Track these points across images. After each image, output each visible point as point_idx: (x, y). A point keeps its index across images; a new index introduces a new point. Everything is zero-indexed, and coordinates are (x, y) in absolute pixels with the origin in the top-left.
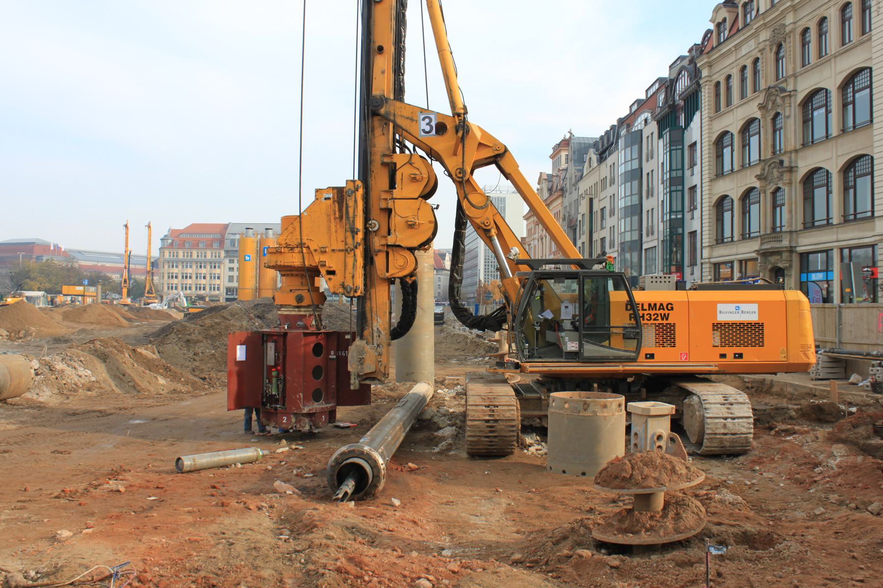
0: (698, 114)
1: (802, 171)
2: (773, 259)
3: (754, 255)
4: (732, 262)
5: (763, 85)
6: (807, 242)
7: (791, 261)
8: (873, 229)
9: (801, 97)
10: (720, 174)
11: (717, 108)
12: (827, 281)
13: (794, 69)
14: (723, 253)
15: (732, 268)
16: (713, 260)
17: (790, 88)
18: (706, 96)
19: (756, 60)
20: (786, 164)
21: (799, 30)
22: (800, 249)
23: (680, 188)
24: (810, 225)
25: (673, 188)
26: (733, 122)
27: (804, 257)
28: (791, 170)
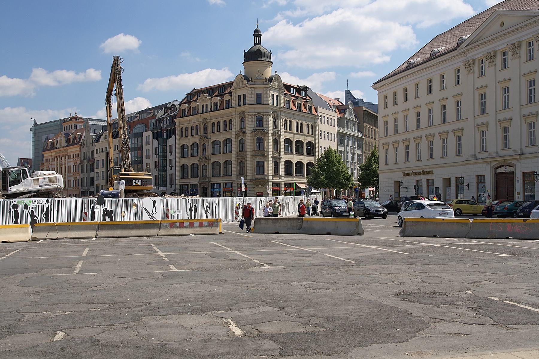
0: (173, 137)
1: (212, 161)
2: (203, 185)
3: (196, 183)
4: (188, 185)
5: (199, 134)
6: (214, 180)
7: (209, 185)
8: (232, 179)
9: (212, 141)
10: (182, 156)
11: (182, 136)
12: (219, 191)
13: (210, 132)
14: (184, 182)
15: (188, 187)
16: (180, 184)
17: (209, 137)
18: (178, 131)
19: (197, 126)
20: (207, 158)
21: (212, 123)
22: (211, 182)
23: (166, 159)
24: (214, 176)
25: (163, 158)
26: (189, 141)
27: (213, 185)
28: (209, 160)
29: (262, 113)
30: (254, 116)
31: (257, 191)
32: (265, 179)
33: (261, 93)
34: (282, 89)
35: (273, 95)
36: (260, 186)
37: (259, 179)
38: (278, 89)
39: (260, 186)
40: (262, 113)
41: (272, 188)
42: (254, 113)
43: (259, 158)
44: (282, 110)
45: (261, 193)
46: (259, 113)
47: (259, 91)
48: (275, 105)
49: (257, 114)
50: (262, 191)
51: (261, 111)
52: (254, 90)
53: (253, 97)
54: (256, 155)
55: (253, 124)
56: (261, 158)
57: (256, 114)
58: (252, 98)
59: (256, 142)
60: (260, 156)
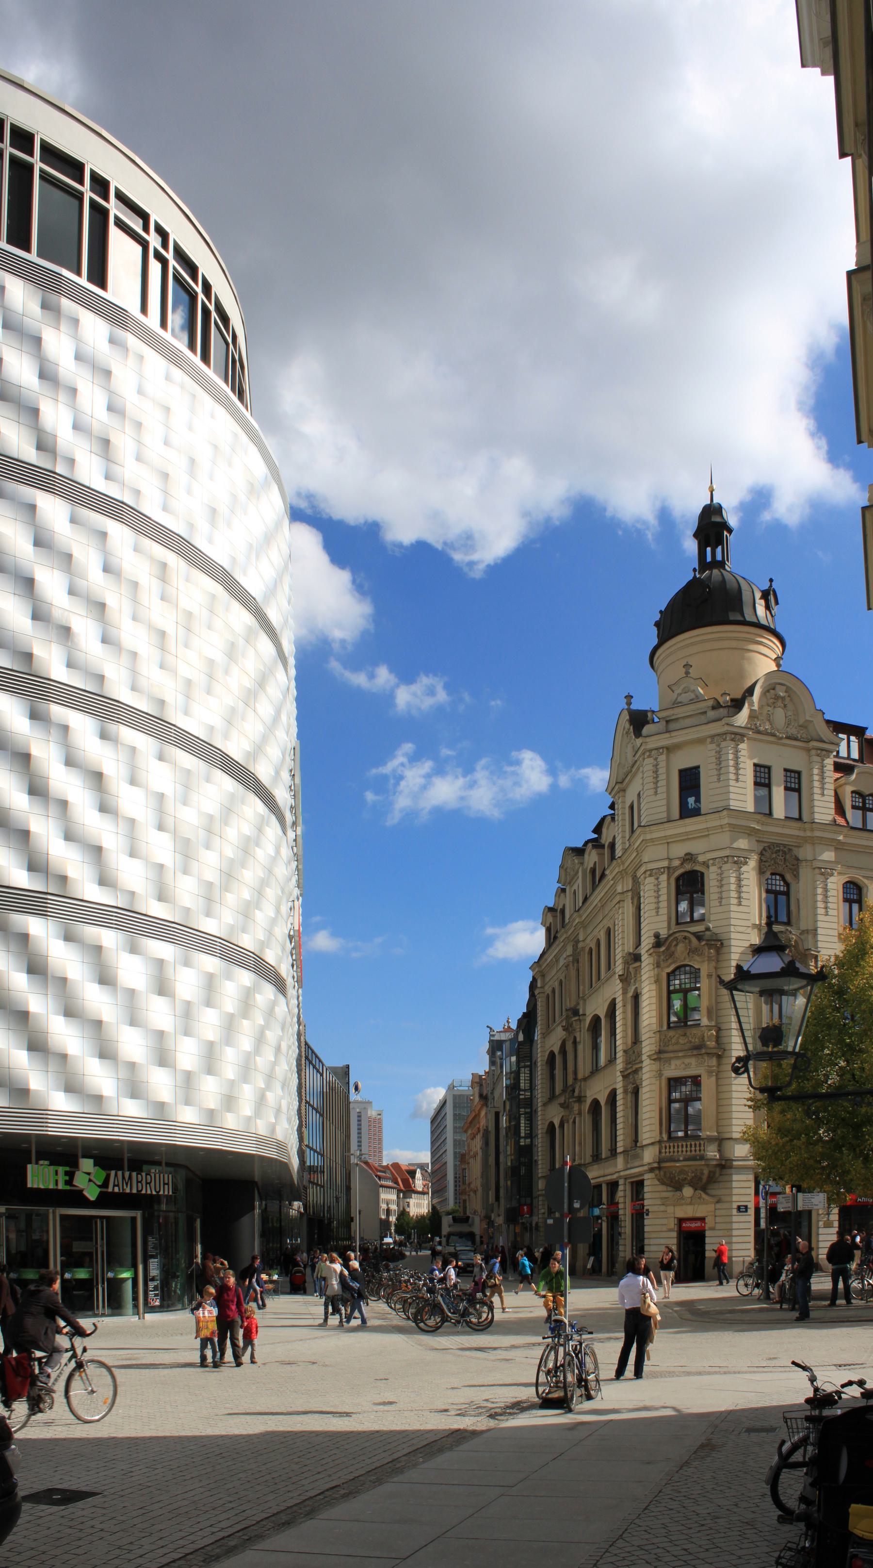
29: (701, 859)
30: (664, 877)
31: (681, 1214)
32: (702, 1158)
33: (698, 767)
34: (824, 742)
35: (769, 768)
36: (688, 1191)
37: (678, 1161)
38: (796, 739)
39: (688, 1191)
40: (701, 859)
41: (752, 1198)
42: (665, 864)
43: (678, 1062)
44: (818, 834)
45: (698, 1224)
46: (689, 857)
47: (684, 760)
48: (779, 811)
49: (676, 868)
50: (699, 1214)
51: (694, 847)
52: (663, 757)
53: (659, 790)
54: (670, 1048)
55: (662, 911)
56: (687, 1061)
57: (676, 863)
58: (658, 797)
59: (670, 993)
60: (680, 1054)
